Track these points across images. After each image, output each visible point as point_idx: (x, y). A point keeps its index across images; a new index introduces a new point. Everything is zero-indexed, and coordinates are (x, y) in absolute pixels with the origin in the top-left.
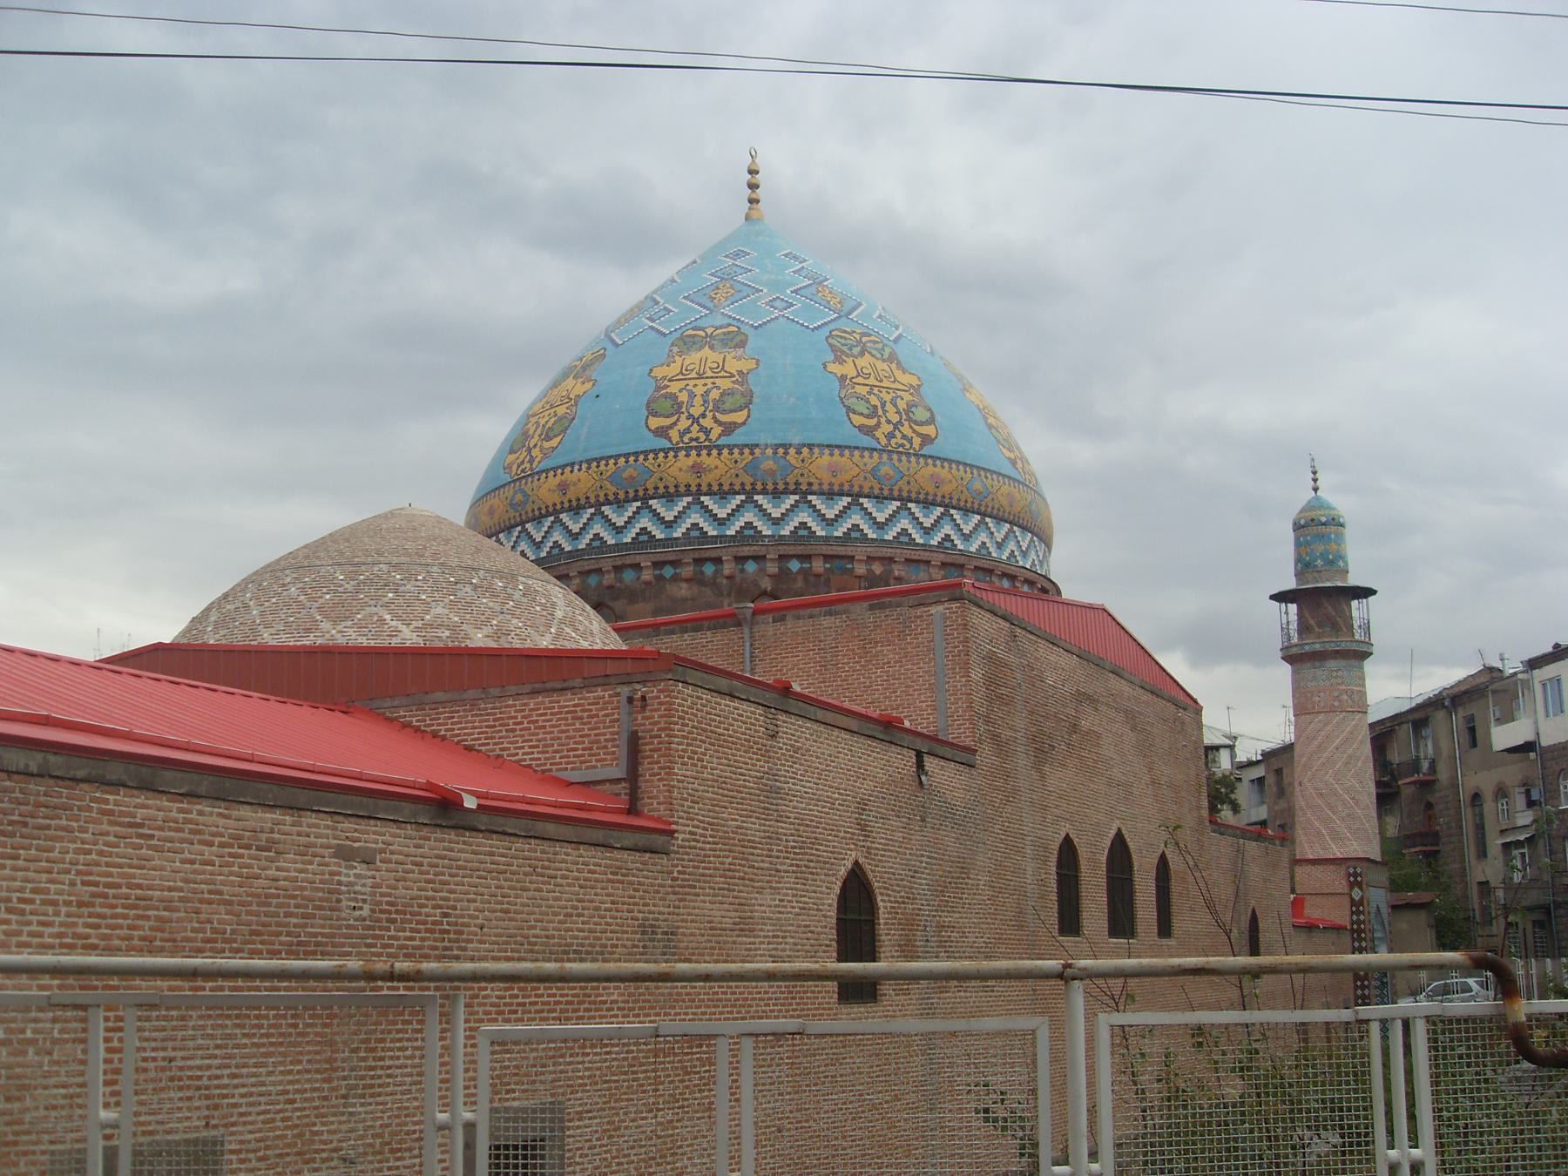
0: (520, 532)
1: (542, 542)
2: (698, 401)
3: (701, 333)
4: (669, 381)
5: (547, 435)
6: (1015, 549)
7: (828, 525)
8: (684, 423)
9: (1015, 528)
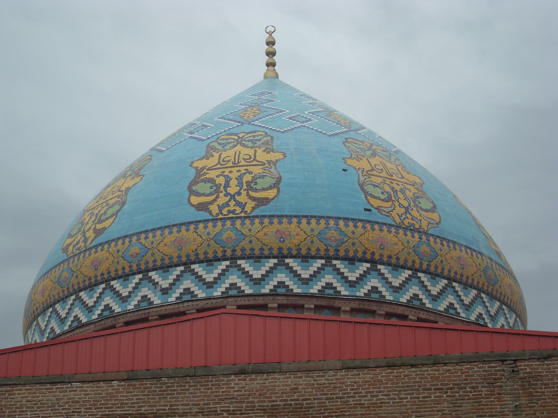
0: (74, 300)
1: (93, 307)
3: (236, 138)
4: (207, 170)
6: (505, 323)
7: (350, 286)
8: (222, 199)
9: (504, 307)
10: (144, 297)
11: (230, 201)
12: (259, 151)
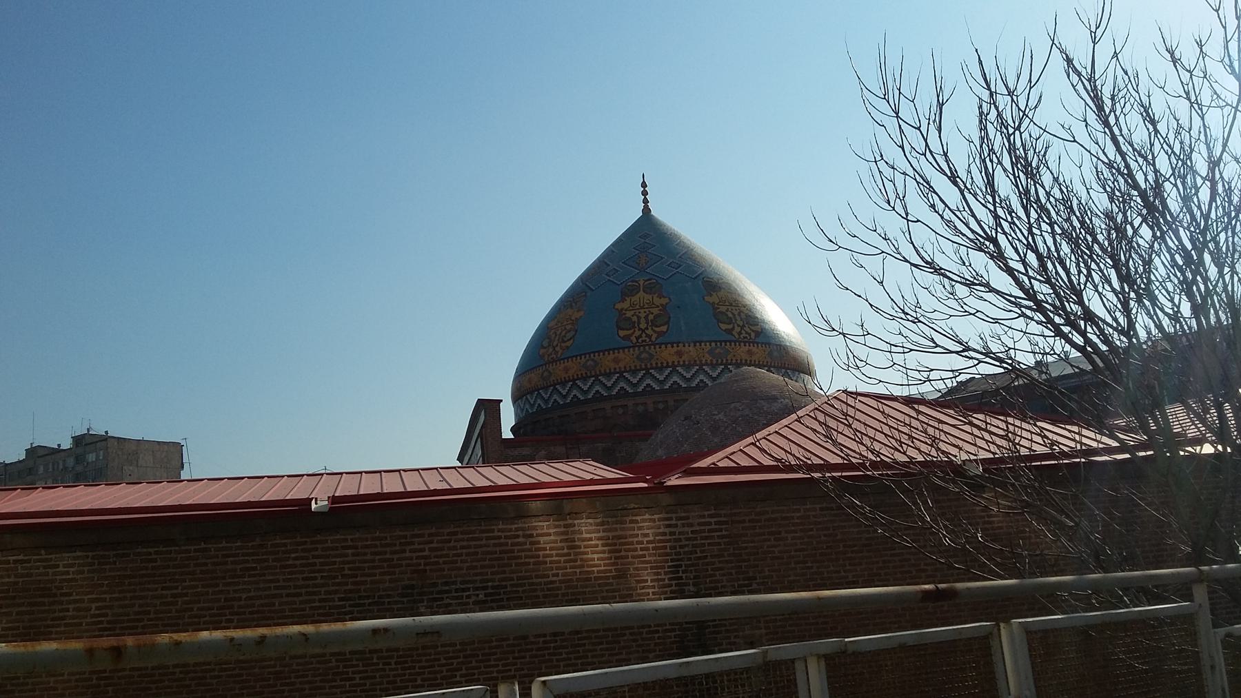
0: (553, 390)
2: (643, 320)
4: (626, 310)
5: (562, 339)
8: (638, 333)
10: (597, 391)
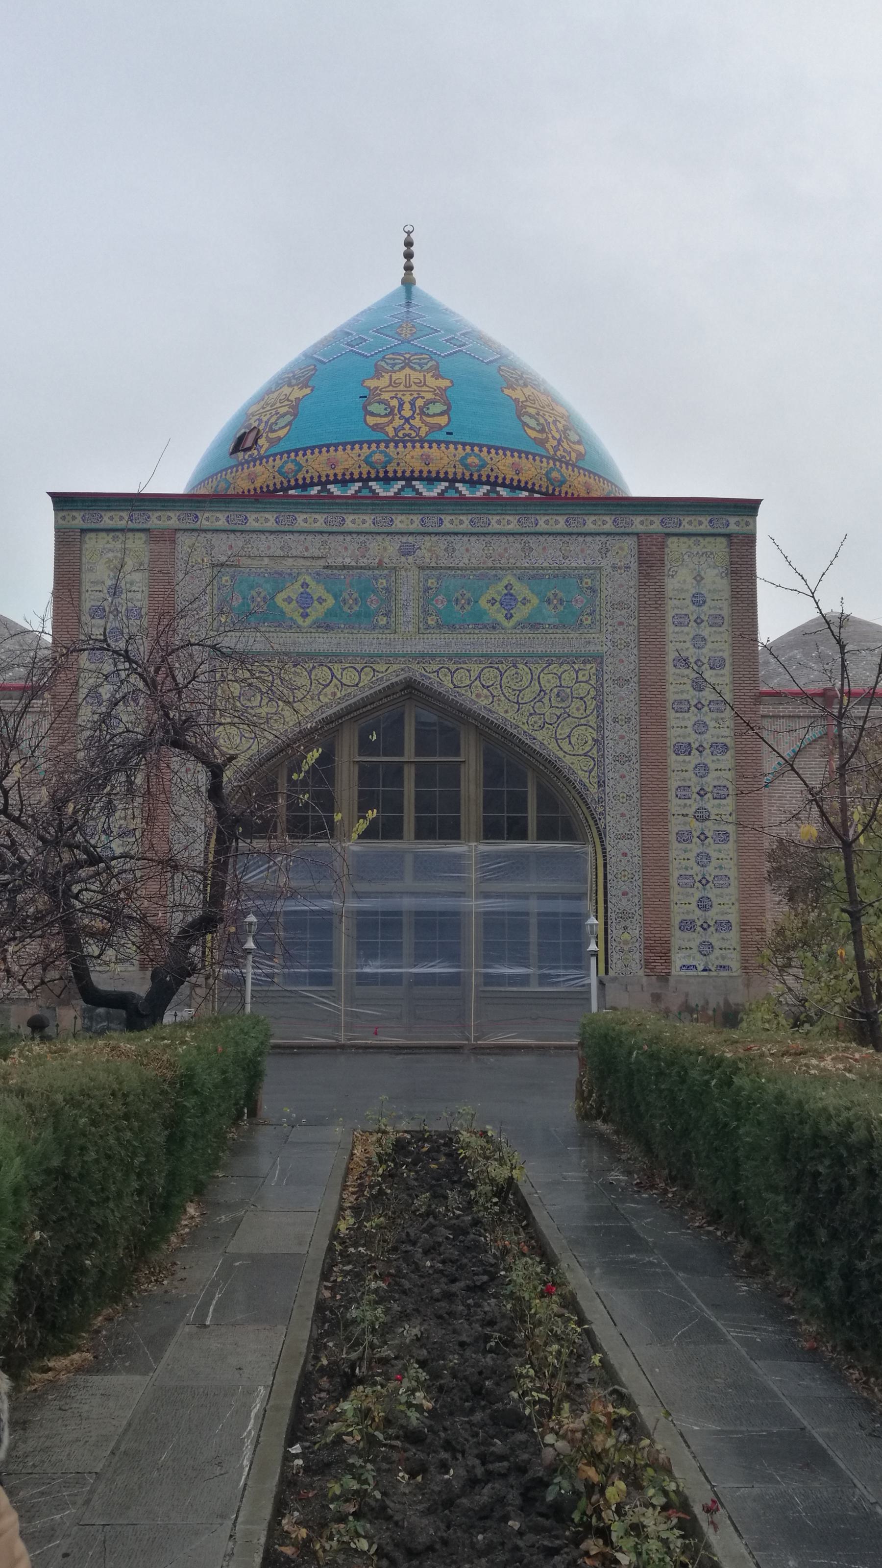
2: (407, 406)
3: (402, 358)
11: (404, 424)
12: (428, 376)
